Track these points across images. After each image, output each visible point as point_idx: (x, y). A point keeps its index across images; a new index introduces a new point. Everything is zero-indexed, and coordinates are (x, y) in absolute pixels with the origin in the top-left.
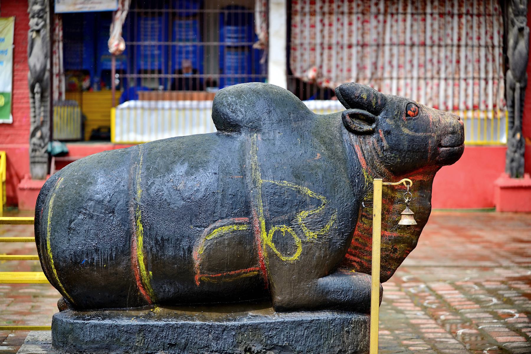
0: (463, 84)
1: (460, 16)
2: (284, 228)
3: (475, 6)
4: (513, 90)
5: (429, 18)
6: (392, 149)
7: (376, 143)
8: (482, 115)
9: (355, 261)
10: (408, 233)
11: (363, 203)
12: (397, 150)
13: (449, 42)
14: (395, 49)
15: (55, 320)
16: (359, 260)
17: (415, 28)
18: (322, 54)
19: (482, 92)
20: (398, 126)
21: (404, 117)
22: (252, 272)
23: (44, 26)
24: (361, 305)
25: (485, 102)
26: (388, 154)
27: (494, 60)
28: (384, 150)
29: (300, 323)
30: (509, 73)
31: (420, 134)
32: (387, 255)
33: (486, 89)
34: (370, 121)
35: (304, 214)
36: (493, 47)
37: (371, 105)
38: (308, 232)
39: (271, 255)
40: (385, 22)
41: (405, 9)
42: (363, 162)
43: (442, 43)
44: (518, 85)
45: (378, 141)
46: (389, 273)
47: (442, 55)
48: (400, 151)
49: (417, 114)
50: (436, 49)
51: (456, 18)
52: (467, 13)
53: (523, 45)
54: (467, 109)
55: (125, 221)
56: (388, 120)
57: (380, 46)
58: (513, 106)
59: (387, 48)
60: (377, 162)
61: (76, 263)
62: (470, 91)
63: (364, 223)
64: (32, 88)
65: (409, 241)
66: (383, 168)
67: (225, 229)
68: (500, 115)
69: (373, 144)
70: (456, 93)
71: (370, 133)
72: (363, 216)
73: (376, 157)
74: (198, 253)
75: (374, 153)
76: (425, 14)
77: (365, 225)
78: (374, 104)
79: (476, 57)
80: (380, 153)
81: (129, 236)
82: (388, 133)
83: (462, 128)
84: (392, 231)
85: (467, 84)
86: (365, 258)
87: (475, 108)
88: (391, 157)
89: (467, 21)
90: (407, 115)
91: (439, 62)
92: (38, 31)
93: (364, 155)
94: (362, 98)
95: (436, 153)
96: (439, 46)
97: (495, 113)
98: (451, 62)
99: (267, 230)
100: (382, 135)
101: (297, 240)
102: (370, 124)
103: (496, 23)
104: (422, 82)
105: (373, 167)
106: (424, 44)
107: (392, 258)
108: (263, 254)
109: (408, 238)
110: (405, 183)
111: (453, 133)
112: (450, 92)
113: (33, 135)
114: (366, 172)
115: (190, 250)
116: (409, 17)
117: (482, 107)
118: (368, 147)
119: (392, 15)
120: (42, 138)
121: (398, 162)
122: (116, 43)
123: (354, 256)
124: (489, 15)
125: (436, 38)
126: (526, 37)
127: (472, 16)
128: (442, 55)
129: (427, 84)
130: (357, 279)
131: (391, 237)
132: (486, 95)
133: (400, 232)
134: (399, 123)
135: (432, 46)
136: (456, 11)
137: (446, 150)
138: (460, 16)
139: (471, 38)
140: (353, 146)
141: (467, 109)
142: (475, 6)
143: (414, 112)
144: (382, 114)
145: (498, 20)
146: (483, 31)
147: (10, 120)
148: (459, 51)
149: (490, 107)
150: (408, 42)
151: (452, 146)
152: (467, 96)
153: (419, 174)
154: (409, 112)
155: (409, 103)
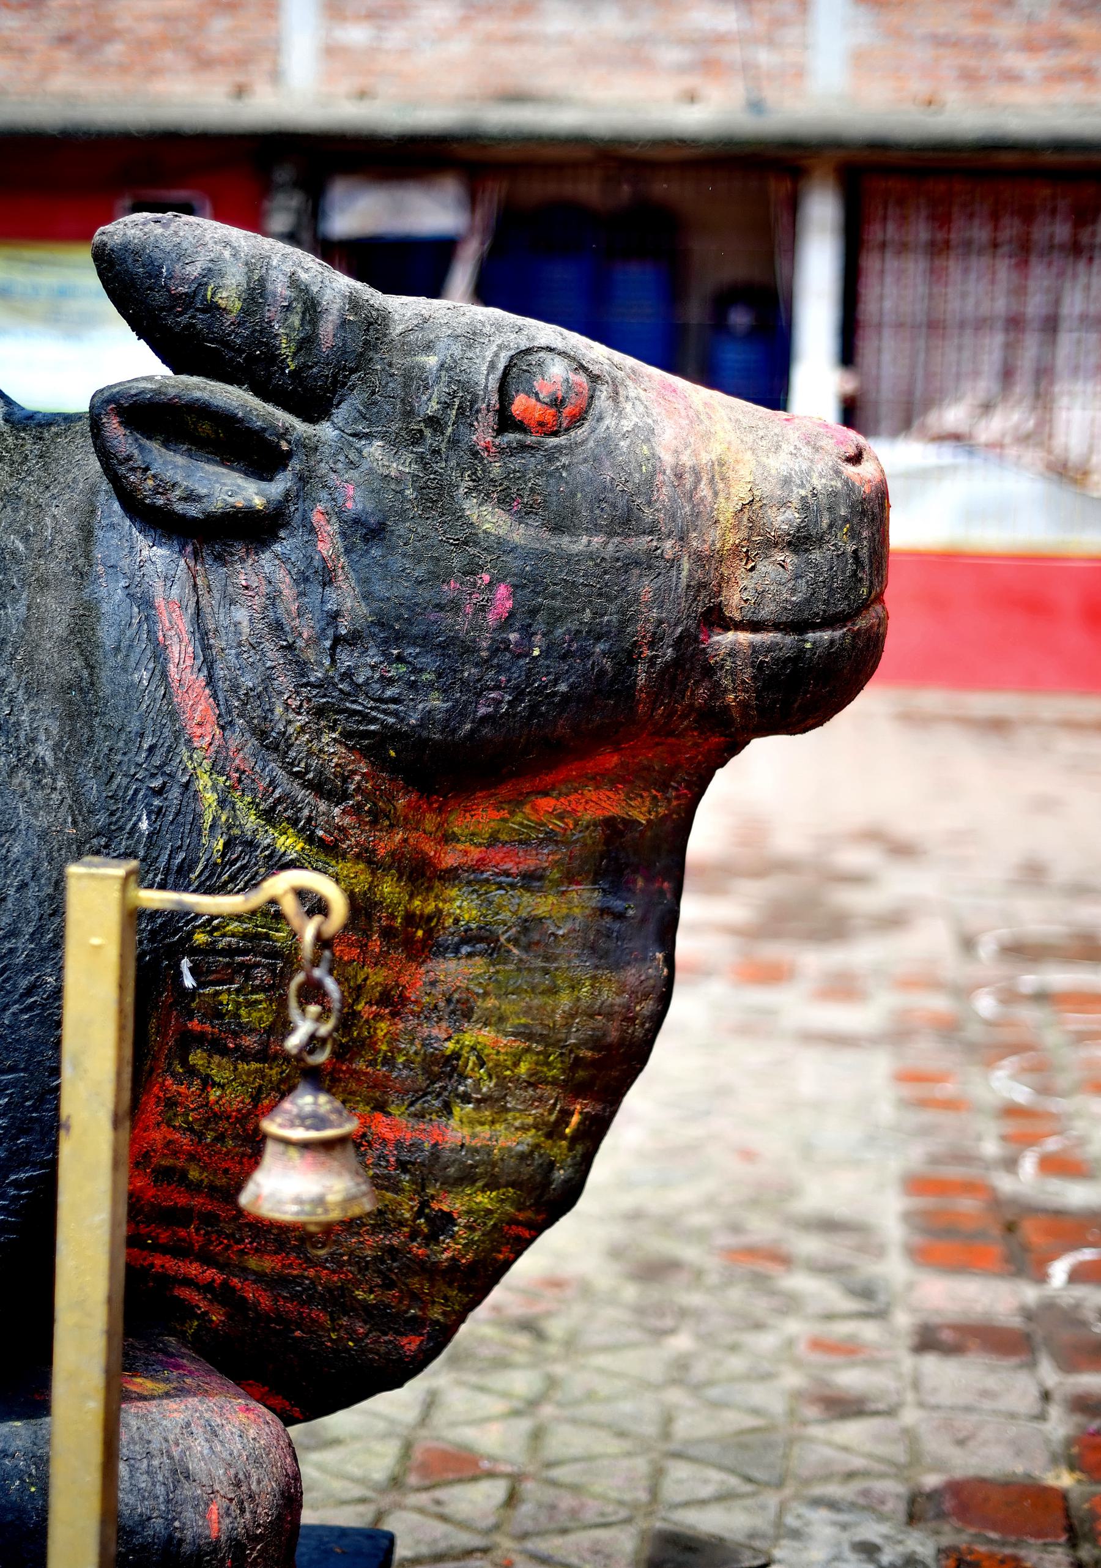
6: (390, 630)
7: (288, 592)
9: (188, 1282)
10: (524, 1128)
11: (185, 964)
12: (424, 640)
16: (211, 1273)
20: (435, 496)
21: (483, 435)
26: (363, 664)
28: (337, 640)
31: (579, 544)
32: (392, 1251)
34: (258, 454)
37: (272, 357)
42: (197, 706)
45: (303, 579)
46: (411, 1344)
48: (456, 649)
49: (579, 419)
56: (375, 449)
60: (288, 716)
63: (207, 1082)
65: (527, 1171)
66: (332, 750)
69: (273, 599)
71: (254, 530)
72: (188, 1041)
73: (284, 681)
75: (273, 656)
77: (214, 1094)
78: (285, 348)
80: (311, 655)
82: (367, 532)
84: (420, 1116)
86: (253, 1263)
90: (506, 422)
94: (212, 308)
95: (690, 661)
105: (271, 743)
107: (429, 1270)
109: (523, 1157)
110: (290, 906)
111: (800, 541)
114: (217, 768)
118: (241, 615)
123: (181, 1251)
131: (416, 1146)
133: (472, 1123)
134: (447, 467)
137: (754, 648)
140: (146, 603)
143: (557, 403)
144: (341, 413)
153: (598, 780)
154: (520, 404)
155: (528, 351)
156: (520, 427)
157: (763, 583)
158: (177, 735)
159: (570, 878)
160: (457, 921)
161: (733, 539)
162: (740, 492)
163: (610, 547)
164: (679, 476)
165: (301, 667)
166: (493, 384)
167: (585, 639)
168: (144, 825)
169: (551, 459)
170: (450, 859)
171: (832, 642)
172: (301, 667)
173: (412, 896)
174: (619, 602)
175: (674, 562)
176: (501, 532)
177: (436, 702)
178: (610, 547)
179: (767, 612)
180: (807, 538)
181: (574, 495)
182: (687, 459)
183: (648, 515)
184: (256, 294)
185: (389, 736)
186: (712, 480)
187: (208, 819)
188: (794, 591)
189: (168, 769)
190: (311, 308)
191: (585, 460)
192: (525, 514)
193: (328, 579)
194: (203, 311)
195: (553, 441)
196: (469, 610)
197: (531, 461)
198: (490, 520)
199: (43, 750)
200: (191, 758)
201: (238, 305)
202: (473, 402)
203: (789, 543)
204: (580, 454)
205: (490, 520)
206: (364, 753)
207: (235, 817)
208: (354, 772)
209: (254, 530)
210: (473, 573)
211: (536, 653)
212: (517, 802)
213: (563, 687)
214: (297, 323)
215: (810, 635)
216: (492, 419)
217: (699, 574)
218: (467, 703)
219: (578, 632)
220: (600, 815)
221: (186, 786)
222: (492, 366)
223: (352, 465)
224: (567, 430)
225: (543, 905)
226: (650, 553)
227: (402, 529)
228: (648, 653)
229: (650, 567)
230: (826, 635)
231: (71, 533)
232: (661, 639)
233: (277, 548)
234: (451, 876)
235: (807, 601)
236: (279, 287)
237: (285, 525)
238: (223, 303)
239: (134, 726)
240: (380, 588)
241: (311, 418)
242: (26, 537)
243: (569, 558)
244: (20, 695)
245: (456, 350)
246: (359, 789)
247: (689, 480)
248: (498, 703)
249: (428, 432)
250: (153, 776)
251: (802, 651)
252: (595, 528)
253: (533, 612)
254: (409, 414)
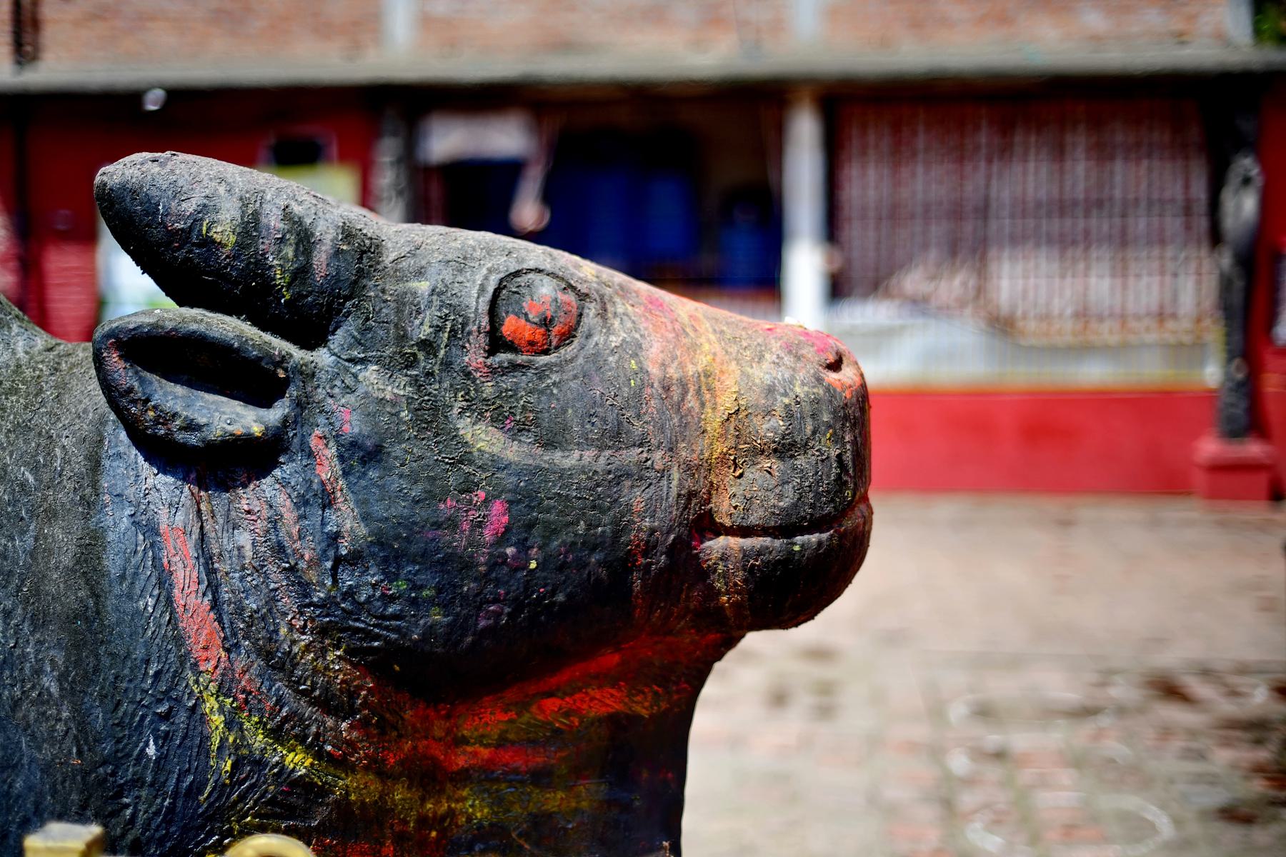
6: (389, 550)
7: (289, 515)
12: (424, 557)
20: (430, 417)
21: (474, 356)
26: (366, 581)
28: (338, 561)
31: (568, 459)
37: (267, 286)
45: (302, 502)
49: (568, 336)
60: (293, 635)
69: (275, 522)
73: (288, 603)
78: (280, 279)
80: (313, 576)
82: (362, 455)
88: (388, 599)
93: (214, 588)
94: (209, 243)
100: (328, 468)
102: (261, 395)
105: (278, 663)
111: (785, 449)
114: (223, 691)
118: (244, 539)
121: (430, 630)
134: (441, 389)
137: (746, 554)
140: (151, 530)
143: (546, 323)
144: (338, 339)
154: (510, 325)
155: (517, 274)
156: (511, 347)
157: (754, 491)
158: (183, 659)
159: (578, 772)
160: (469, 819)
161: (720, 448)
162: (726, 403)
163: (602, 461)
164: (667, 389)
165: (304, 589)
166: (484, 307)
167: (581, 550)
168: (151, 751)
169: (541, 375)
170: (461, 761)
171: (820, 543)
172: (304, 589)
173: (423, 800)
174: (611, 513)
175: (664, 473)
176: (495, 450)
177: (437, 617)
178: (602, 461)
179: (754, 519)
180: (793, 444)
181: (564, 411)
182: (673, 372)
183: (638, 429)
184: (250, 227)
185: (392, 651)
186: (698, 392)
187: (216, 740)
188: (780, 497)
189: (174, 694)
190: (304, 239)
191: (575, 377)
192: (520, 430)
193: (327, 501)
194: (199, 246)
195: (543, 359)
196: (466, 526)
197: (523, 380)
198: (484, 438)
199: (50, 683)
200: (197, 682)
201: (233, 239)
202: (464, 325)
203: (775, 450)
204: (570, 371)
205: (484, 438)
206: (369, 669)
207: (243, 738)
208: (361, 688)
210: (469, 491)
211: (533, 565)
212: (523, 706)
213: (560, 598)
214: (291, 254)
215: (799, 539)
216: (483, 340)
217: (689, 483)
218: (467, 618)
219: (574, 544)
220: (603, 711)
221: (193, 709)
222: (482, 289)
223: (349, 390)
224: (557, 347)
225: (554, 800)
226: (643, 465)
227: (397, 450)
228: (642, 561)
229: (641, 479)
230: (814, 538)
231: (79, 463)
232: (655, 547)
233: (277, 472)
234: (463, 777)
235: (795, 505)
236: (273, 220)
237: (285, 450)
238: (218, 238)
239: (139, 653)
240: (378, 509)
241: (309, 345)
242: (35, 469)
243: (562, 474)
244: (26, 627)
245: (447, 275)
246: (365, 704)
247: (676, 393)
248: (498, 615)
249: (421, 356)
250: (159, 701)
251: (792, 553)
252: (587, 442)
253: (530, 526)
254: (402, 338)
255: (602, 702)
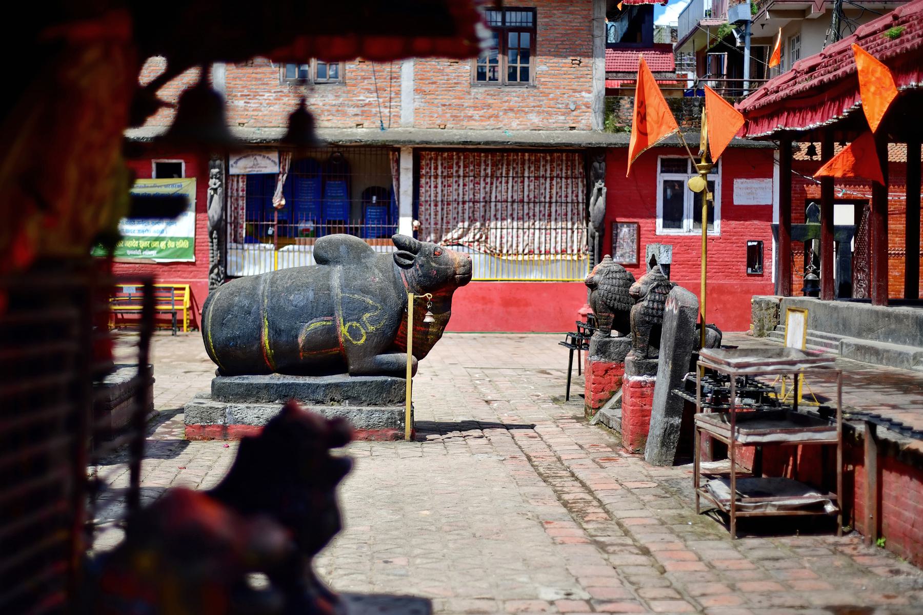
0: (553, 232)
1: (552, 179)
2: (355, 324)
3: (564, 171)
4: (593, 237)
5: (526, 179)
6: (424, 276)
8: (569, 258)
13: (543, 199)
14: (499, 205)
15: (213, 382)
17: (515, 188)
18: (442, 209)
19: (569, 239)
20: (428, 262)
22: (336, 351)
23: (220, 186)
24: (401, 372)
25: (572, 247)
27: (578, 214)
29: (365, 383)
30: (590, 224)
33: (572, 237)
34: (410, 258)
35: (367, 315)
36: (578, 203)
38: (369, 325)
39: (347, 340)
40: (492, 184)
41: (507, 174)
43: (537, 200)
44: (597, 234)
47: (537, 210)
48: (430, 277)
50: (531, 205)
51: (548, 180)
52: (557, 176)
53: (601, 200)
54: (557, 253)
55: (258, 318)
57: (487, 202)
58: (593, 251)
59: (493, 204)
60: (414, 284)
61: (226, 346)
62: (559, 239)
64: (211, 234)
67: (318, 324)
68: (583, 257)
70: (548, 239)
71: (410, 266)
74: (301, 339)
76: (524, 177)
79: (564, 211)
81: (260, 328)
82: (421, 266)
83: (471, 263)
85: (557, 233)
87: (563, 252)
89: (557, 183)
91: (534, 215)
92: (215, 190)
96: (534, 202)
97: (579, 256)
98: (544, 215)
99: (344, 325)
101: (363, 331)
103: (580, 184)
104: (521, 231)
105: (413, 287)
106: (522, 201)
108: (342, 340)
112: (543, 239)
113: (212, 272)
115: (297, 337)
116: (511, 179)
117: (569, 251)
119: (497, 178)
120: (218, 274)
122: (278, 200)
124: (575, 178)
125: (532, 196)
126: (604, 195)
127: (561, 178)
128: (537, 210)
129: (524, 233)
130: (400, 356)
132: (573, 242)
135: (528, 203)
136: (548, 175)
138: (552, 179)
139: (561, 196)
141: (557, 253)
142: (564, 171)
145: (582, 182)
146: (570, 191)
147: (193, 260)
148: (550, 207)
149: (575, 252)
150: (510, 199)
151: (464, 274)
152: (556, 243)
157: (460, 270)
198: (434, 264)
205: (434, 264)
209: (410, 266)
255: (443, 294)
